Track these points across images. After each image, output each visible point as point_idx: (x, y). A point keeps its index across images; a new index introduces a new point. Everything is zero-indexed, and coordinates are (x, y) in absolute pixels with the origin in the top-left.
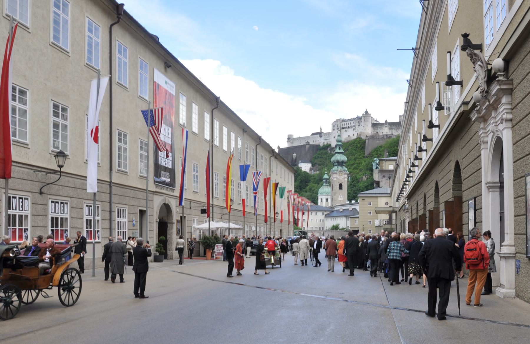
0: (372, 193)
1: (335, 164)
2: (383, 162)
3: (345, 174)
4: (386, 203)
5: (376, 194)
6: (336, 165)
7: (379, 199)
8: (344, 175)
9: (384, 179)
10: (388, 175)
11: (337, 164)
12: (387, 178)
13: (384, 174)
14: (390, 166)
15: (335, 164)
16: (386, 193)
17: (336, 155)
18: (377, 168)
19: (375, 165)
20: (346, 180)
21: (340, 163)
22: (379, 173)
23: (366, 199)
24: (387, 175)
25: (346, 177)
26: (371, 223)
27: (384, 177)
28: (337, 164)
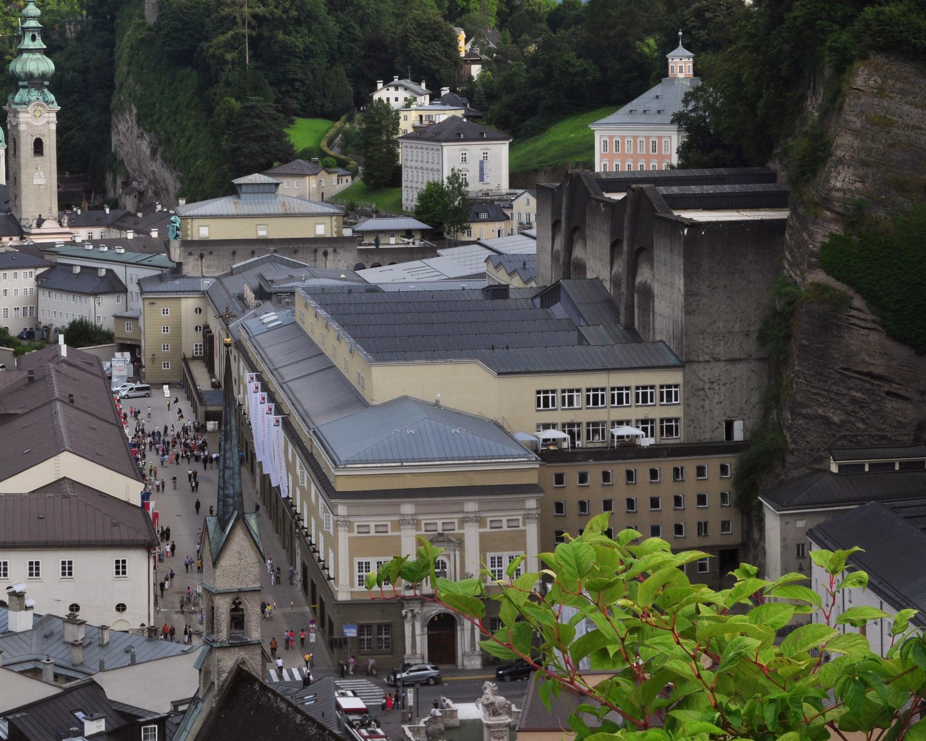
0: (169, 289)
1: (20, 83)
2: (189, 221)
3: (49, 112)
4: (196, 309)
5: (177, 292)
6: (24, 87)
7: (183, 302)
8: (47, 115)
9: (191, 259)
10: (199, 252)
11: (25, 83)
12: (196, 256)
13: (191, 249)
14: (201, 228)
15: (20, 83)
16: (196, 289)
17: (25, 55)
18: (177, 236)
19: (173, 231)
20: (53, 127)
21: (34, 81)
22: (181, 246)
23: (157, 302)
24: (197, 251)
25: (51, 119)
26: (168, 349)
27: (190, 254)
28: (25, 83)
